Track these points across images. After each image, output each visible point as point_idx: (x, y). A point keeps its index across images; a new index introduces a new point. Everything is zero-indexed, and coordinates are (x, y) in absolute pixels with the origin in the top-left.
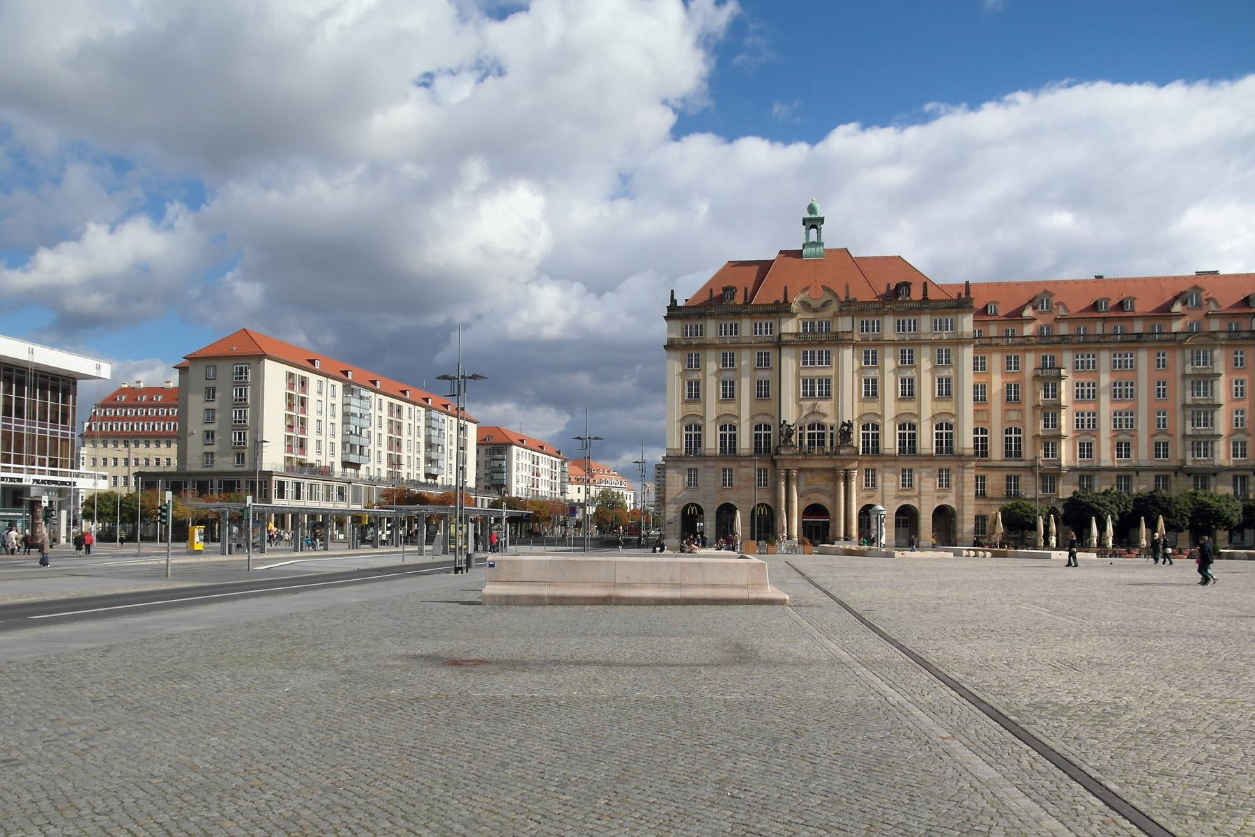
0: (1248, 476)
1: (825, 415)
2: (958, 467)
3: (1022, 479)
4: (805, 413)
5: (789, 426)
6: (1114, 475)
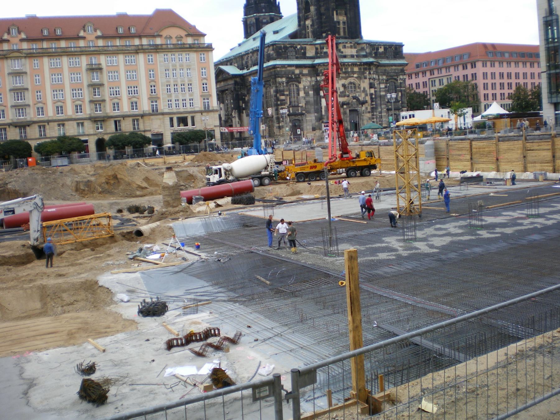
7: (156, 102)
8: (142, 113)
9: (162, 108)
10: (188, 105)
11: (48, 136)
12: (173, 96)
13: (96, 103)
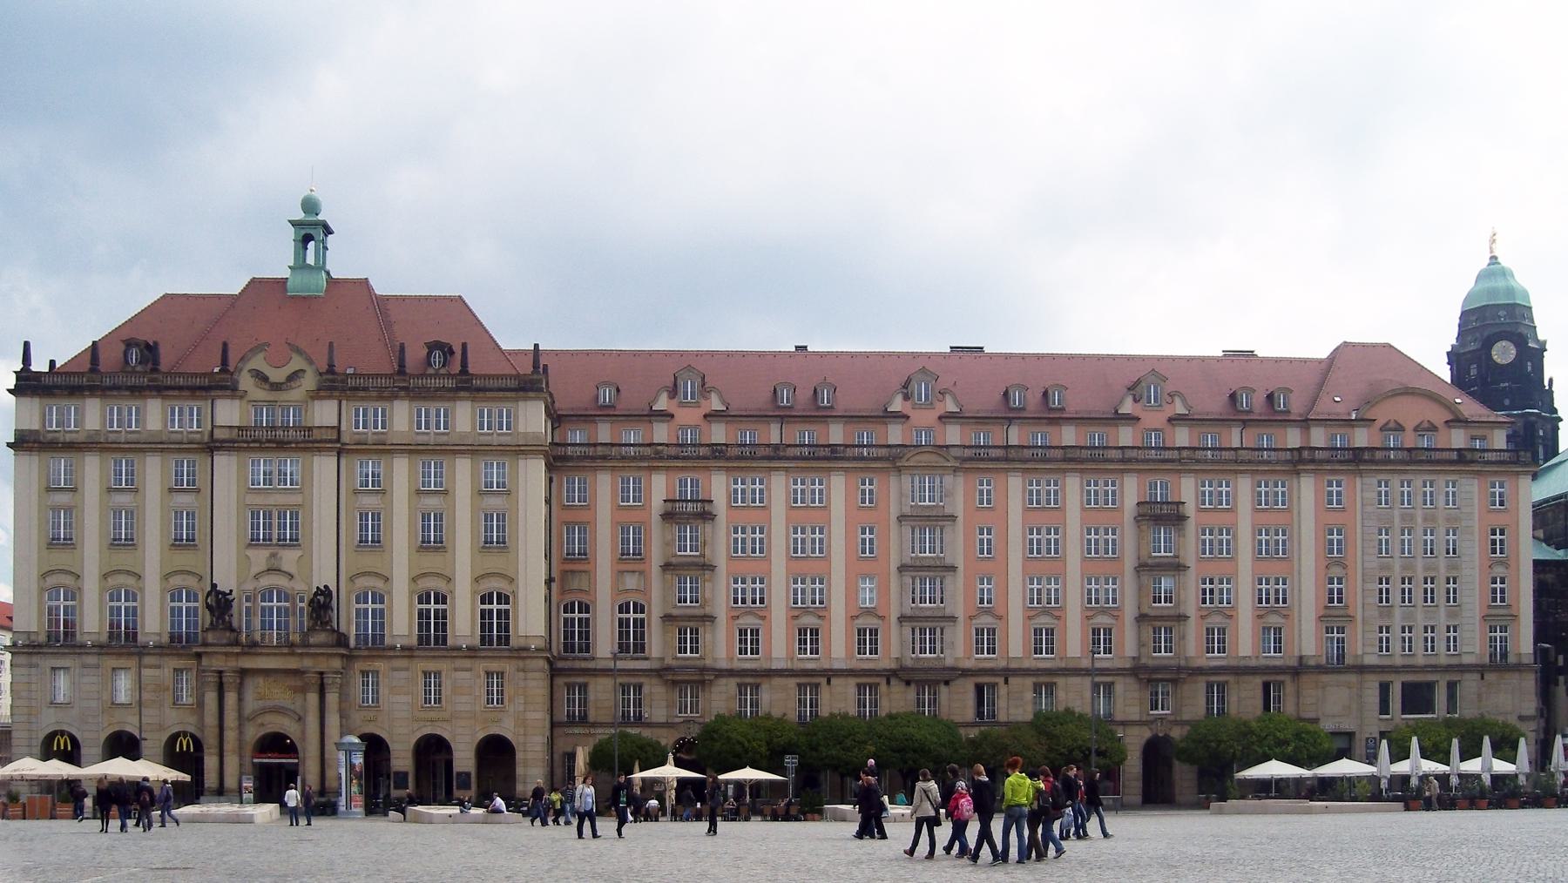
3: (645, 690)
6: (792, 682)
7: (1341, 630)
8: (1293, 663)
9: (1360, 652)
10: (1441, 646)
11: (1002, 717)
12: (1397, 612)
13: (1158, 624)
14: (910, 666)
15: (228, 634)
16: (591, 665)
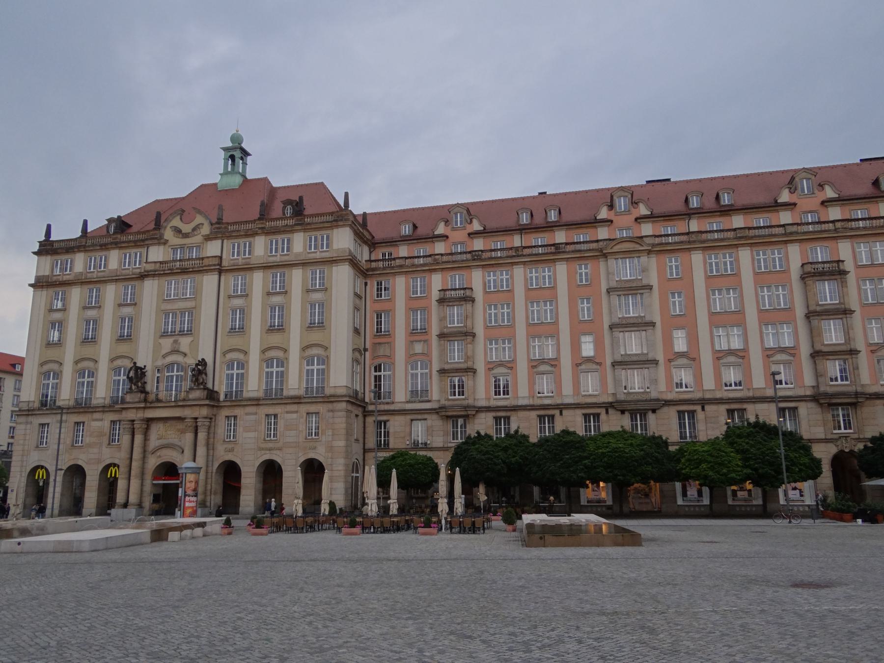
0: (695, 411)
1: (185, 355)
2: (329, 411)
4: (164, 352)
5: (141, 369)
14: (623, 399)
15: (139, 395)
16: (392, 407)
